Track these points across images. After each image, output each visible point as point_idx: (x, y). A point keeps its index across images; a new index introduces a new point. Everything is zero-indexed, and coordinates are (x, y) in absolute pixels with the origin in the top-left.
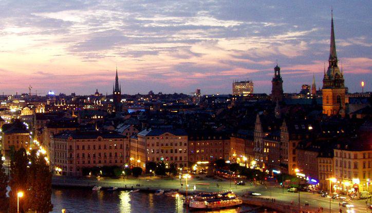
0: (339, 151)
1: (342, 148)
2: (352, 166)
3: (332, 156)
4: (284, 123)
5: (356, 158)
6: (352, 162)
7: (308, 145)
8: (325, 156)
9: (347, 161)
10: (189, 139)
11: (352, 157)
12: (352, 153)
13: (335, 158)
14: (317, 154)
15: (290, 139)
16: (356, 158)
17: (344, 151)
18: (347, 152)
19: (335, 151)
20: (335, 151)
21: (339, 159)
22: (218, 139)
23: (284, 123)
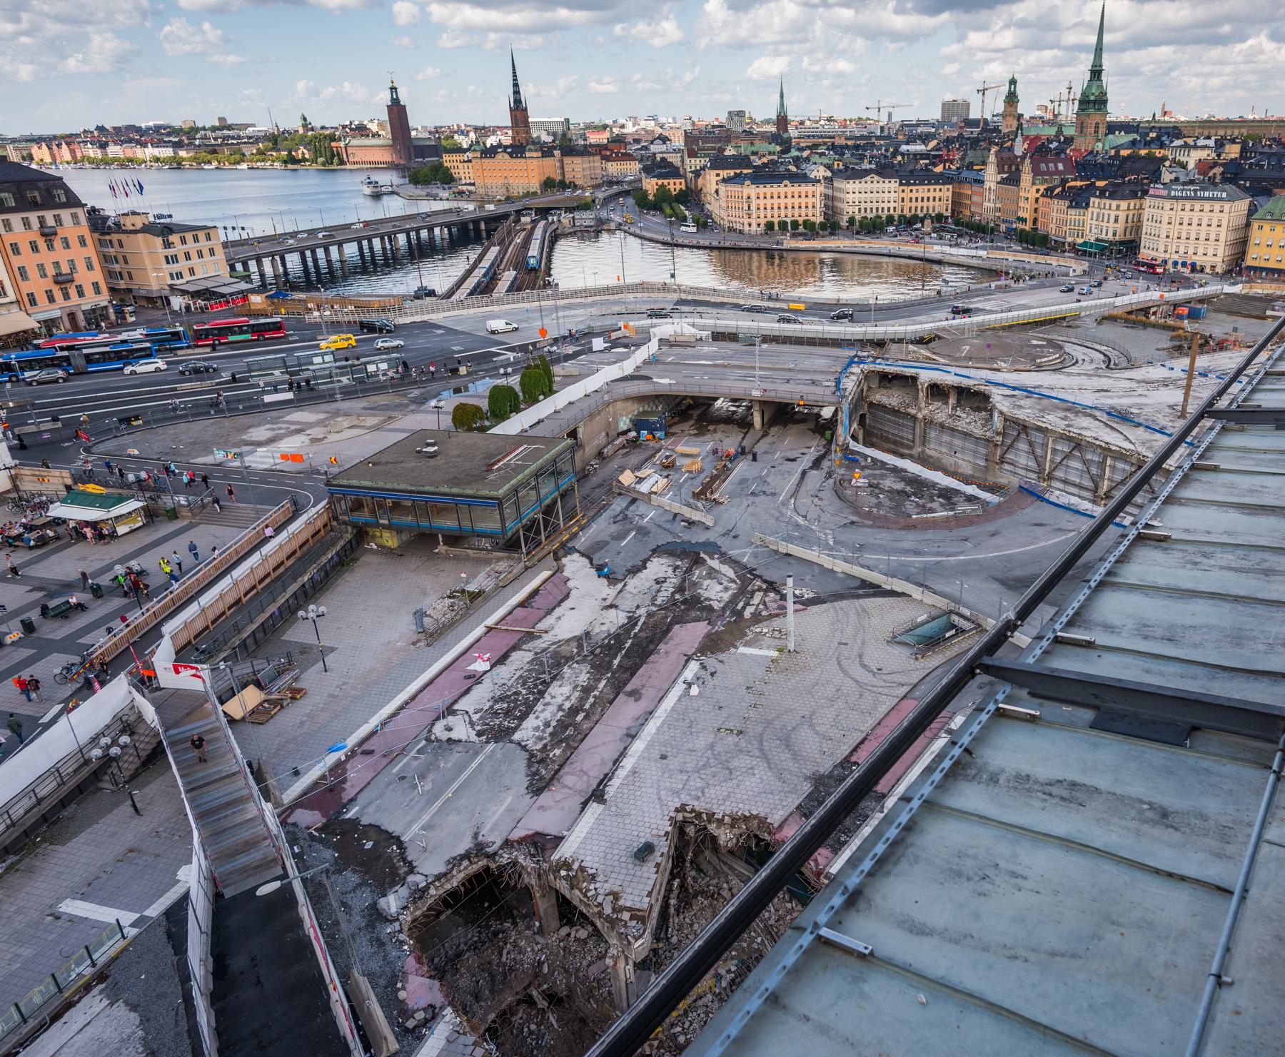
0: (1097, 200)
1: (1102, 196)
2: (1112, 220)
3: (1087, 205)
4: (1028, 161)
5: (1118, 207)
6: (1113, 214)
7: (1057, 191)
8: (1078, 206)
9: (1106, 212)
10: (901, 184)
11: (1114, 207)
12: (1114, 203)
13: (1090, 210)
14: (1067, 203)
15: (1034, 184)
16: (1118, 207)
17: (1104, 201)
18: (1108, 202)
19: (1092, 199)
20: (1092, 199)
21: (1096, 211)
22: (937, 183)
23: (1028, 161)
